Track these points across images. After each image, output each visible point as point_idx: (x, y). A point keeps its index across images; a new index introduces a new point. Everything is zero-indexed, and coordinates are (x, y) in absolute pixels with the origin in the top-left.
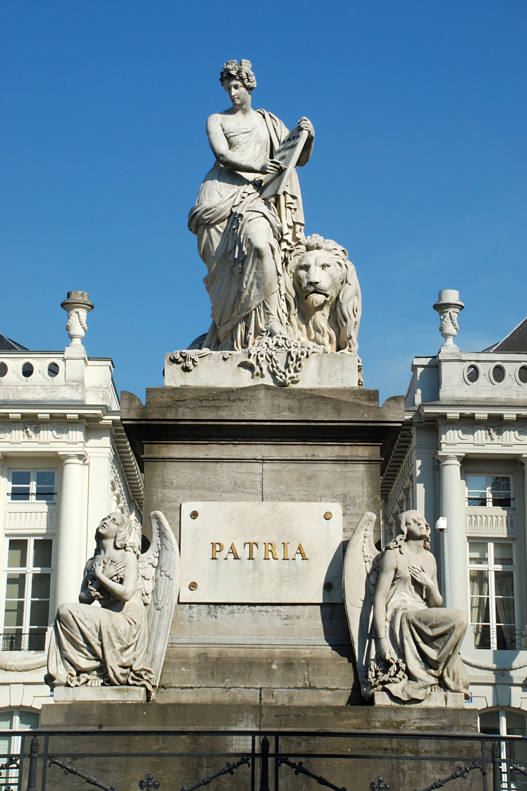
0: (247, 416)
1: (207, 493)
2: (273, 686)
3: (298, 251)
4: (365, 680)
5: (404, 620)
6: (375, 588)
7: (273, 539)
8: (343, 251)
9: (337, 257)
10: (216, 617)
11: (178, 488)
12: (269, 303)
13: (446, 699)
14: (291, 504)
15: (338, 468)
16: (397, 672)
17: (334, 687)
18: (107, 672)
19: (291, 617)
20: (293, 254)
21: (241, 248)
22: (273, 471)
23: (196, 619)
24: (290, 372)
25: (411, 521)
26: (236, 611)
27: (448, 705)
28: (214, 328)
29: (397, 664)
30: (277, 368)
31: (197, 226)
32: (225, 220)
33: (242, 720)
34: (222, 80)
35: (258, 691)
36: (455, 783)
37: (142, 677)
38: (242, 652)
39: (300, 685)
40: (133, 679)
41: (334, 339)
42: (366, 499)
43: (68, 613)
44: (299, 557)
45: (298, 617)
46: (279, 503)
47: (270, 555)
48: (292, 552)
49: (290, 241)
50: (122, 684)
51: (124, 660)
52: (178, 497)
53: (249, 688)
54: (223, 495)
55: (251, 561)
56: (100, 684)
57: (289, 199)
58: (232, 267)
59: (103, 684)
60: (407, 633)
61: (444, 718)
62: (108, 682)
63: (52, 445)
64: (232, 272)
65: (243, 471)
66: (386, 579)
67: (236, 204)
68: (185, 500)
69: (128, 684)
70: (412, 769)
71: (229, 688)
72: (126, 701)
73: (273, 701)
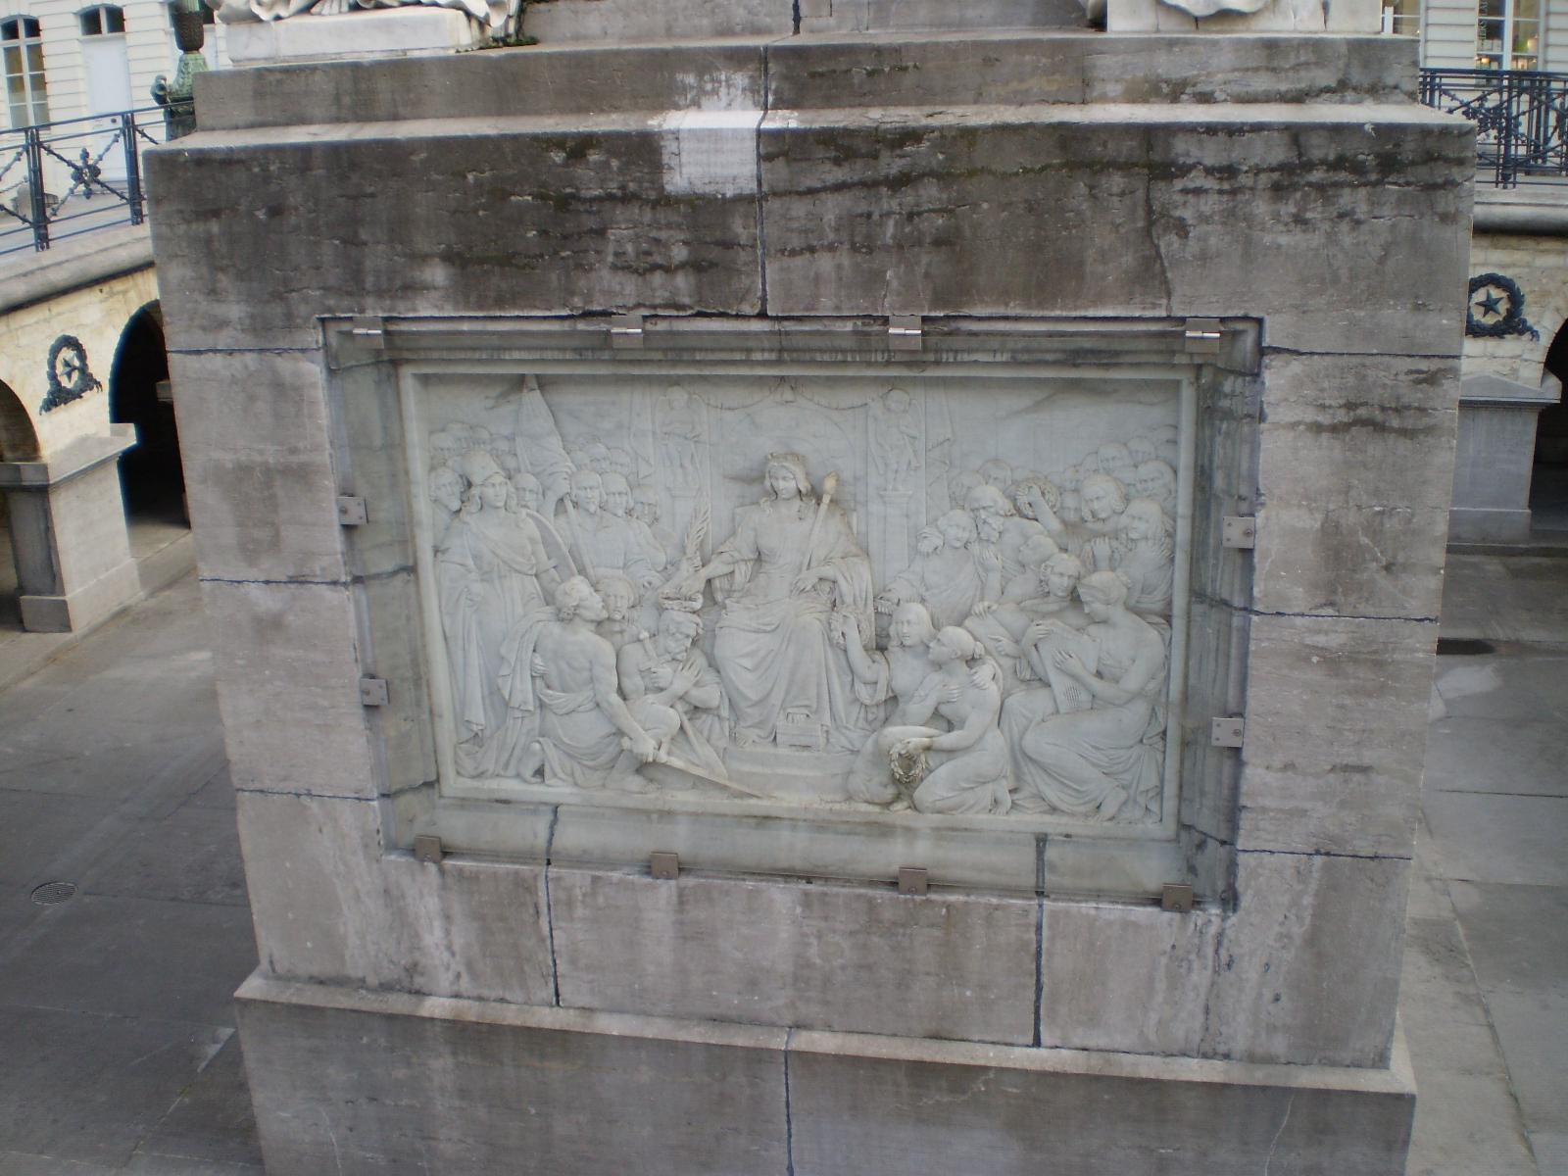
27: (1331, 25)
33: (715, 92)
36: (1334, 256)
56: (345, 8)
61: (1320, 63)
70: (1205, 219)
72: (404, 51)
73: (832, 21)
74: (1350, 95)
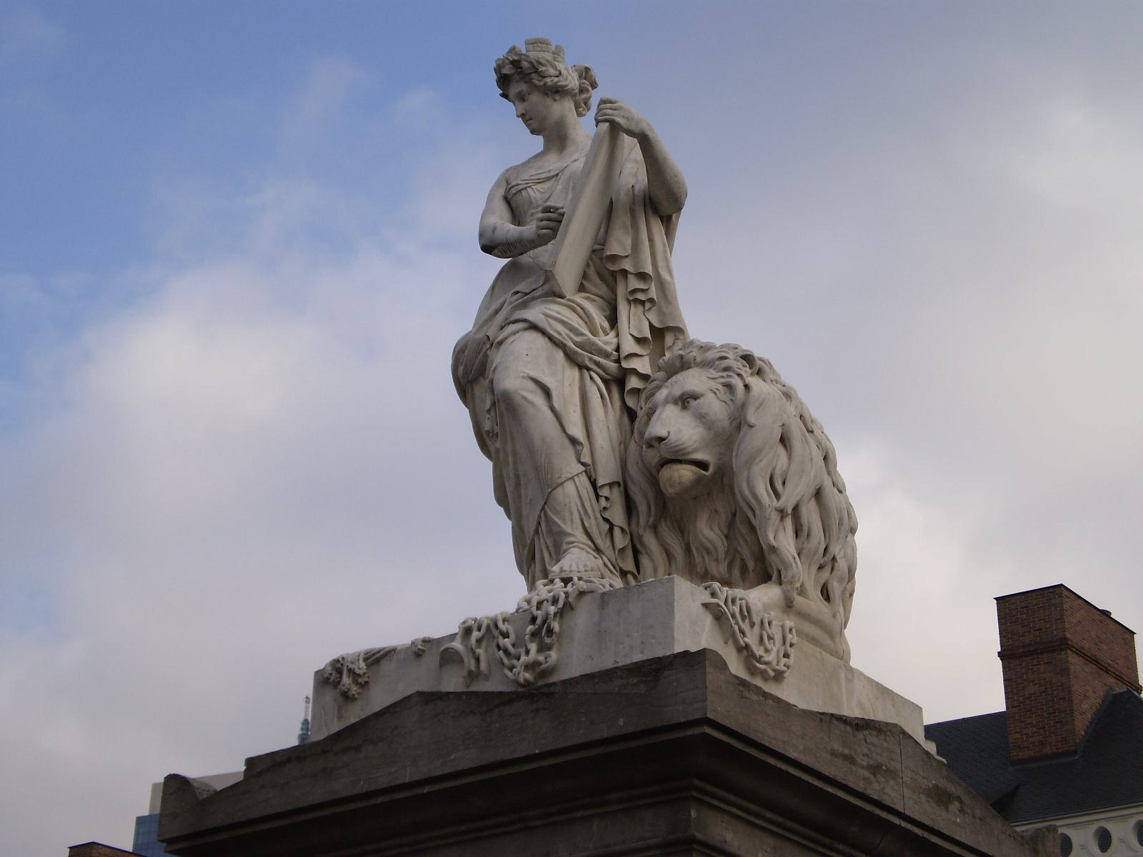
9: (724, 374)
12: (557, 513)
57: (634, 283)
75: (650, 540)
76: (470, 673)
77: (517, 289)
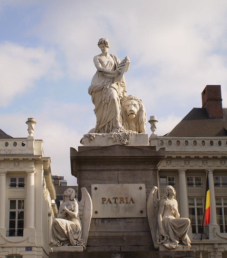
0: (113, 155)
1: (100, 181)
2: (125, 245)
3: (125, 100)
4: (155, 242)
5: (168, 223)
6: (158, 212)
7: (123, 196)
8: (140, 100)
10: (104, 223)
11: (90, 180)
13: (183, 248)
14: (128, 184)
15: (144, 172)
16: (167, 240)
17: (145, 245)
18: (70, 241)
19: (129, 222)
20: (123, 101)
21: (107, 99)
22: (122, 173)
23: (97, 223)
24: (126, 140)
25: (169, 189)
26: (111, 221)
28: (97, 126)
29: (167, 237)
30: (121, 139)
31: (92, 92)
32: (101, 90)
34: (98, 45)
35: (120, 247)
37: (81, 243)
38: (113, 234)
39: (134, 244)
40: (78, 244)
41: (138, 129)
42: (153, 182)
43: (57, 222)
44: (131, 202)
45: (132, 222)
46: (124, 184)
47: (122, 202)
48: (129, 201)
49: (122, 97)
50: (75, 245)
51: (76, 237)
52: (90, 183)
53: (116, 246)
54: (105, 182)
55: (115, 204)
58: (104, 106)
59: (69, 245)
60: (169, 227)
62: (70, 245)
63: (23, 169)
64: (104, 107)
65: (112, 174)
66: (162, 209)
67: (105, 84)
68: (92, 184)
69: (77, 245)
71: (110, 246)
74: (187, 257)
75: (124, 123)
76: (115, 141)
77: (108, 80)
